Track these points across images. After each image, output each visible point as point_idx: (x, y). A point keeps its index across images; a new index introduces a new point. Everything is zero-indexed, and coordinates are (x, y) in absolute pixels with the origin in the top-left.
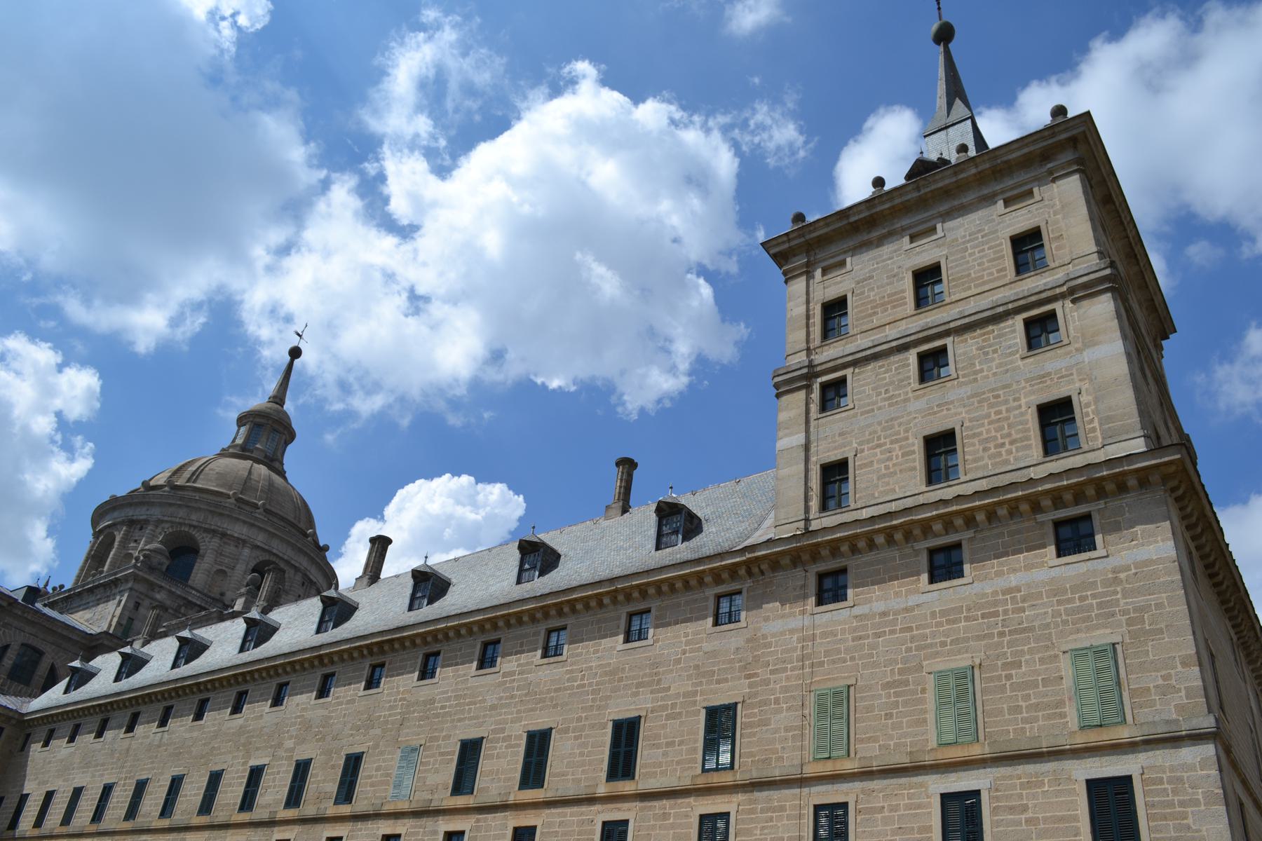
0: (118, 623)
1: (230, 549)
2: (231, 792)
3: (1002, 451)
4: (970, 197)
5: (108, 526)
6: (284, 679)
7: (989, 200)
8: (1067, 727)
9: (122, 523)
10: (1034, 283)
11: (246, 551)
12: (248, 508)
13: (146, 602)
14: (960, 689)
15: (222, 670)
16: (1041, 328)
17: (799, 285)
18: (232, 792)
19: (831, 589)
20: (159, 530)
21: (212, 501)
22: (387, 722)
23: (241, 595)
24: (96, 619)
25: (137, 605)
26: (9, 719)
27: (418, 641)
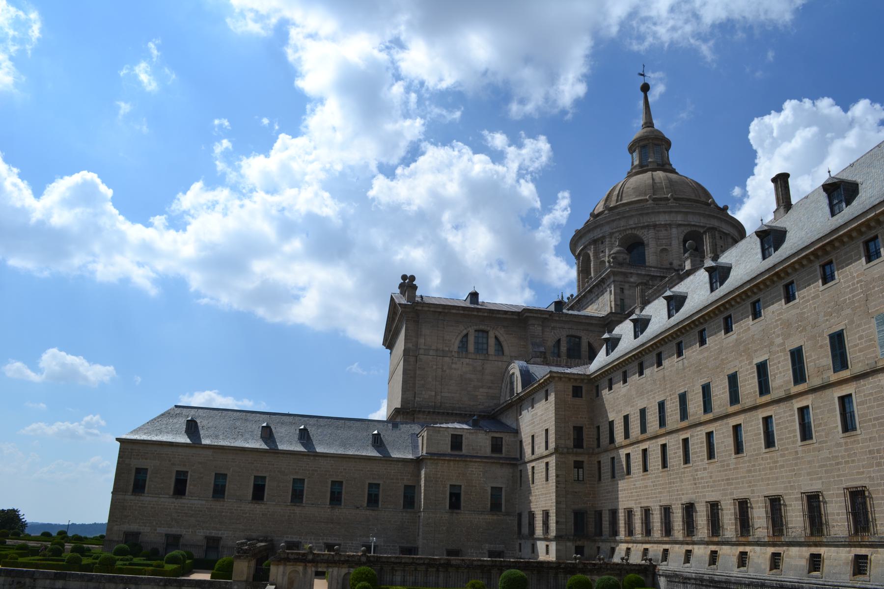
0: (616, 305)
1: (663, 233)
2: (749, 385)
5: (582, 250)
6: (755, 298)
9: (590, 244)
11: (674, 231)
12: (663, 202)
13: (626, 286)
15: (706, 307)
18: (749, 384)
20: (613, 240)
21: (638, 208)
22: (853, 302)
23: (687, 258)
24: (602, 306)
25: (622, 290)
26: (582, 380)
27: (854, 234)
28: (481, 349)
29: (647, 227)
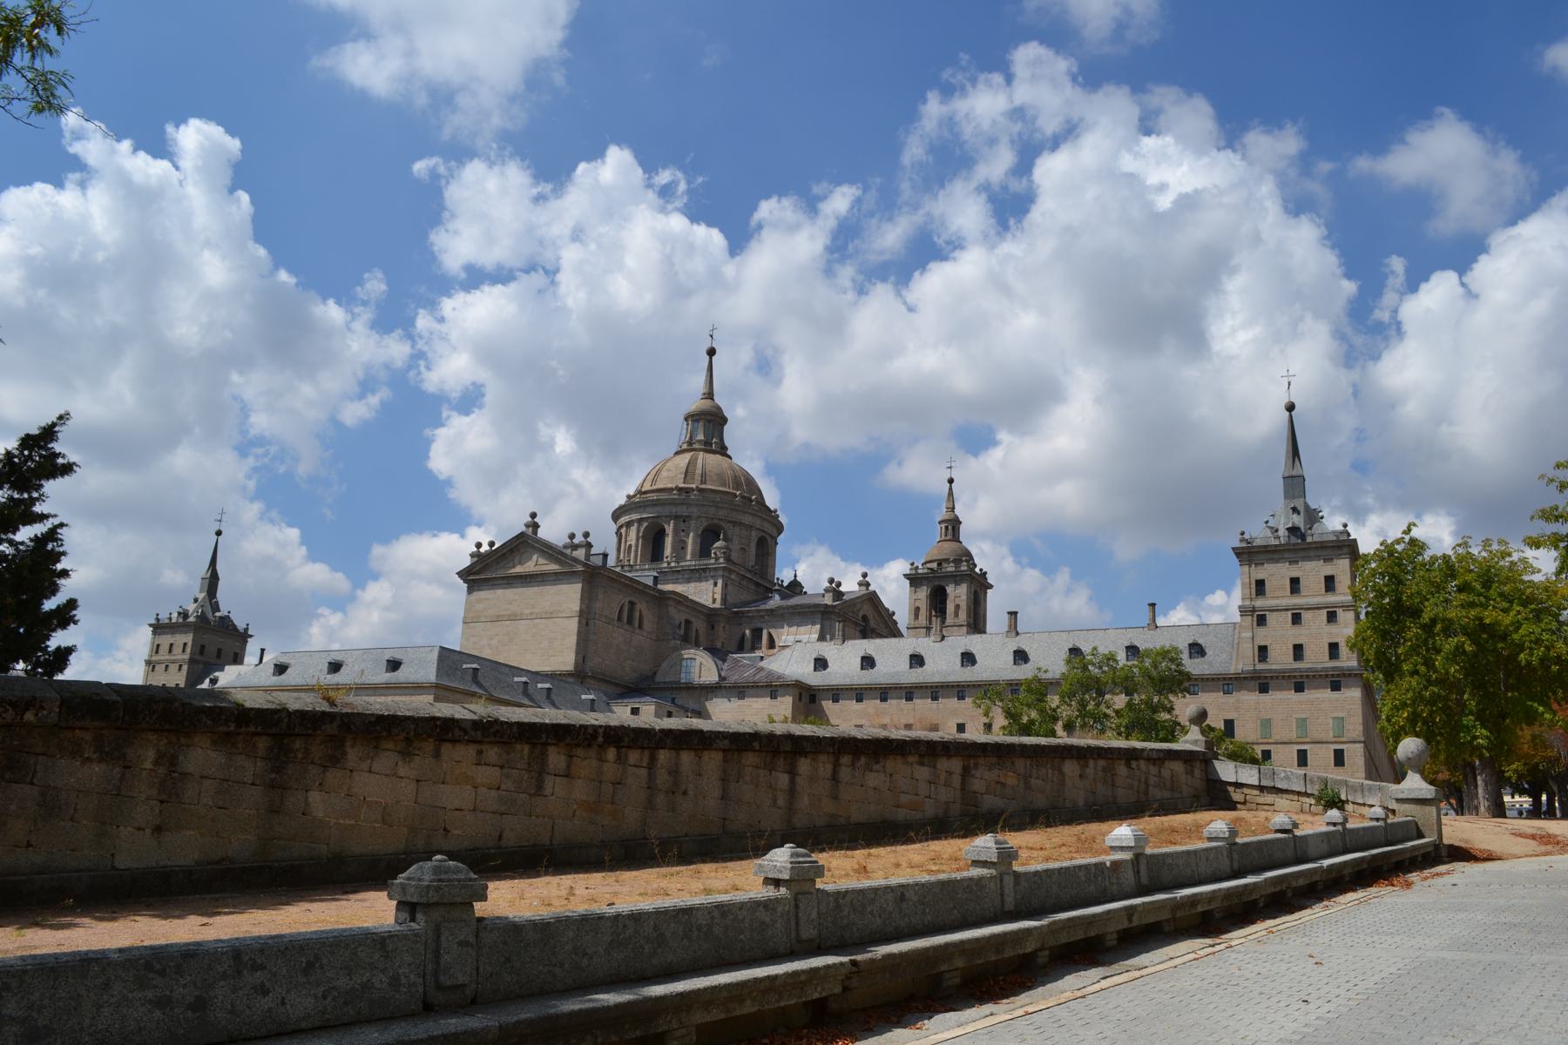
3: (1316, 657)
4: (1312, 553)
7: (1318, 558)
8: (1330, 736)
10: (1331, 599)
11: (754, 533)
14: (1302, 723)
16: (1332, 617)
17: (1246, 568)
19: (1264, 689)
28: (630, 622)
29: (734, 523)
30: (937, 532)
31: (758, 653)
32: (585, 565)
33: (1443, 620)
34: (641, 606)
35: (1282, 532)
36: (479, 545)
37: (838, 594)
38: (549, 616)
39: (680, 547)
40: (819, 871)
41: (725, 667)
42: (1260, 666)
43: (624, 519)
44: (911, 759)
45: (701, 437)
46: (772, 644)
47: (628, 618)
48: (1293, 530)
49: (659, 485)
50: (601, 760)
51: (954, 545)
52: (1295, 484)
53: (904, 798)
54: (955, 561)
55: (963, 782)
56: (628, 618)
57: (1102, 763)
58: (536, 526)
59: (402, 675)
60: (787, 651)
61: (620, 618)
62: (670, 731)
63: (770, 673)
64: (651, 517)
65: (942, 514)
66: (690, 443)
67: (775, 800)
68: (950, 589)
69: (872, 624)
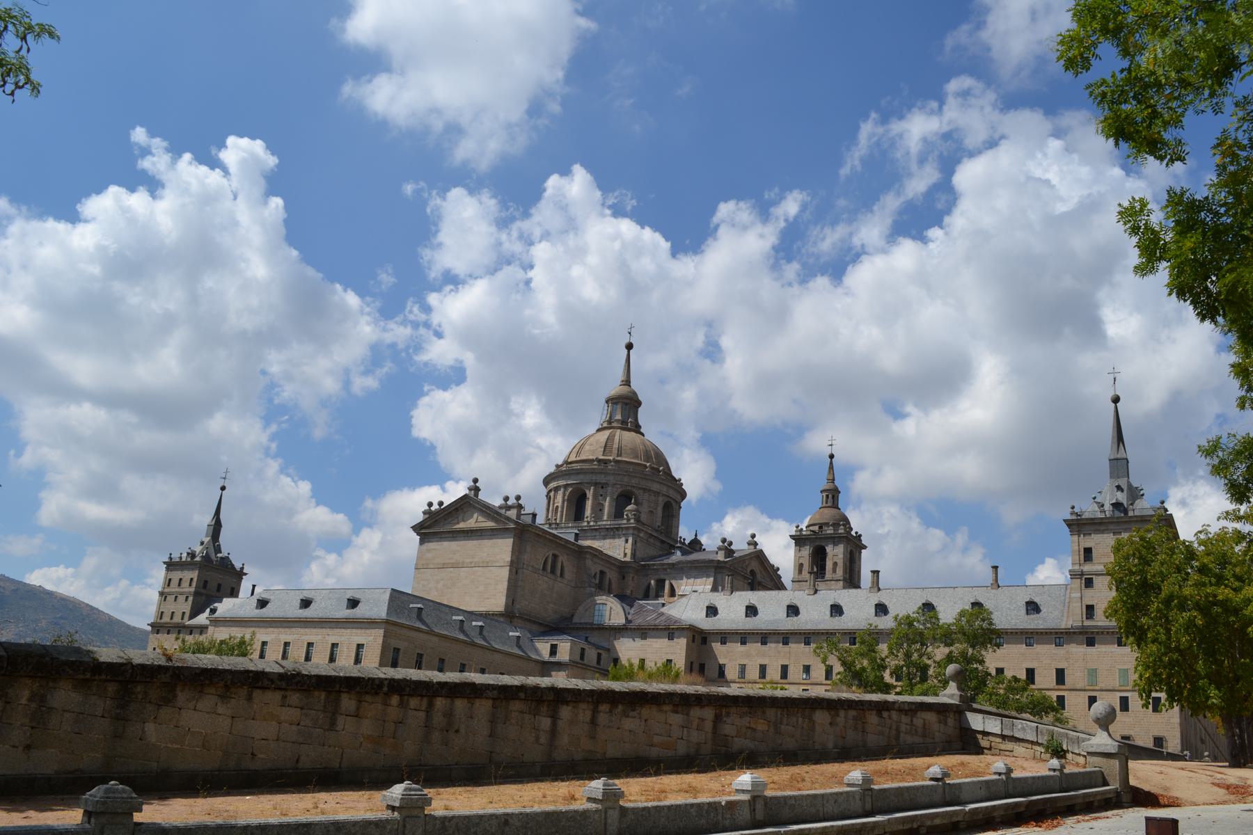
11: (661, 499)
19: (1091, 643)
28: (553, 571)
29: (644, 490)
30: (818, 500)
31: (661, 601)
32: (516, 523)
33: (1178, 597)
34: (563, 558)
35: (1107, 507)
36: (430, 504)
37: (729, 552)
38: (486, 565)
39: (598, 509)
40: (428, 801)
41: (632, 611)
42: (1088, 623)
43: (552, 485)
44: (666, 708)
45: (619, 417)
46: (673, 593)
47: (552, 567)
48: (1117, 506)
49: (583, 457)
50: (386, 704)
51: (833, 511)
52: (1119, 466)
53: (656, 739)
54: (833, 525)
55: (715, 727)
56: (552, 567)
57: (852, 713)
58: (477, 490)
59: (359, 612)
60: (684, 600)
61: (544, 569)
62: (446, 683)
63: (669, 618)
64: (576, 483)
65: (824, 484)
66: (610, 422)
67: (537, 739)
68: (829, 549)
69: (759, 577)
